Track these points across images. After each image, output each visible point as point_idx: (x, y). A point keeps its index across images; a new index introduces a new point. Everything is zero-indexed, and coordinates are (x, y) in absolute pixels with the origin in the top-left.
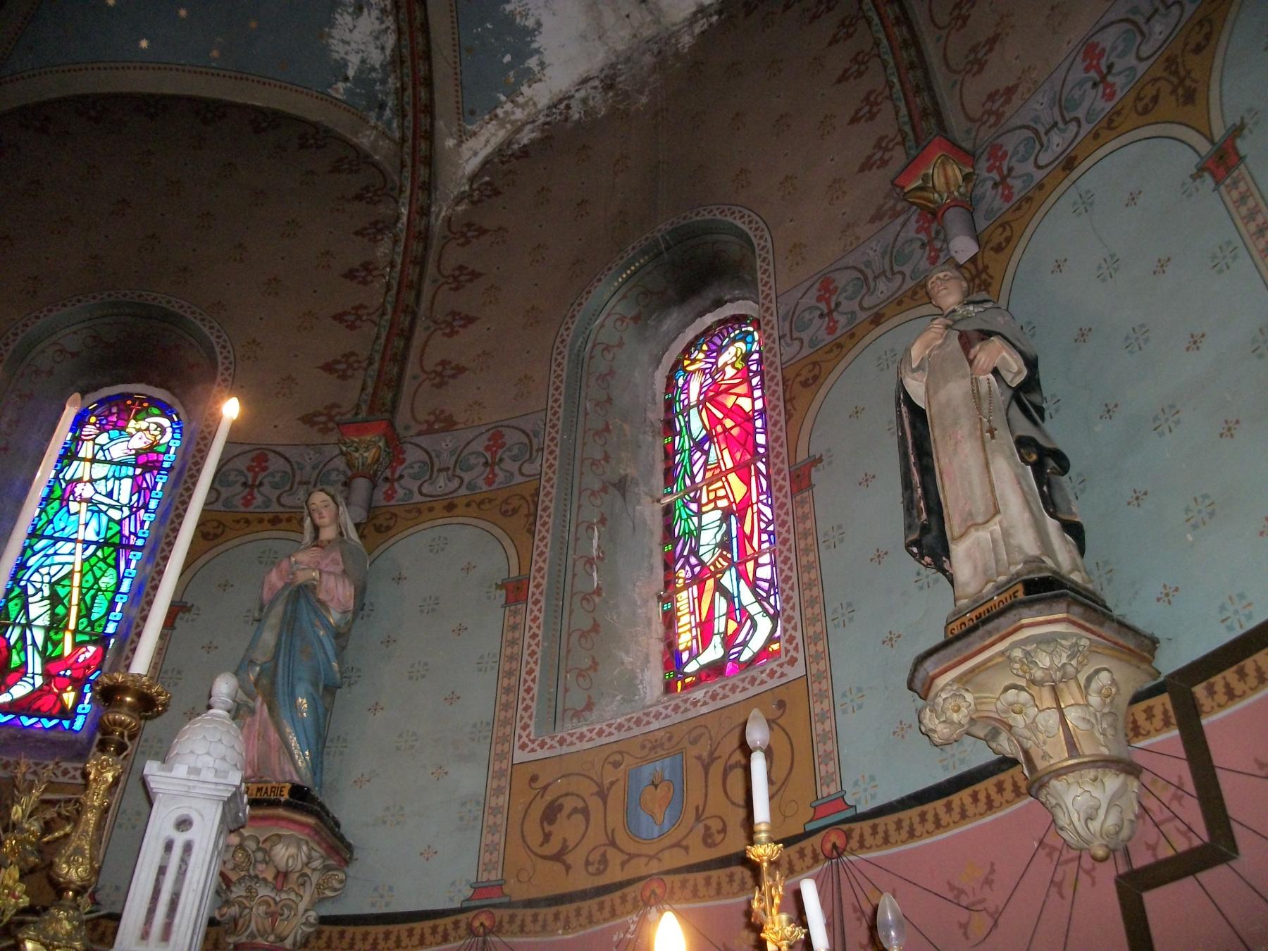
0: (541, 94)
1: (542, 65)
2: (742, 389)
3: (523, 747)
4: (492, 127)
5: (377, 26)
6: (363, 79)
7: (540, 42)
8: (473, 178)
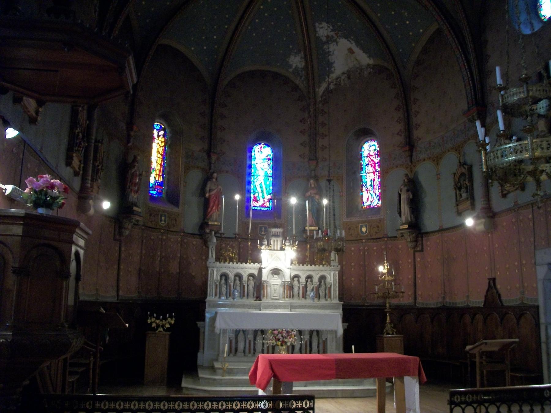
0: (334, 76)
1: (335, 70)
2: (374, 156)
3: (345, 219)
4: (324, 84)
5: (300, 60)
6: (296, 68)
7: (334, 65)
8: (322, 97)
